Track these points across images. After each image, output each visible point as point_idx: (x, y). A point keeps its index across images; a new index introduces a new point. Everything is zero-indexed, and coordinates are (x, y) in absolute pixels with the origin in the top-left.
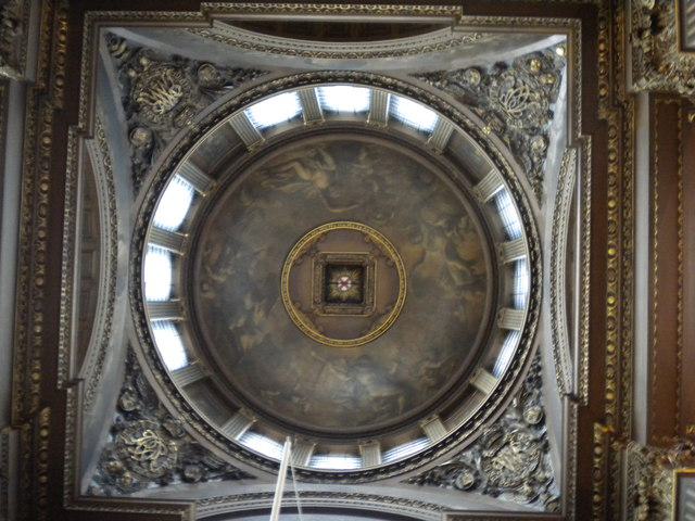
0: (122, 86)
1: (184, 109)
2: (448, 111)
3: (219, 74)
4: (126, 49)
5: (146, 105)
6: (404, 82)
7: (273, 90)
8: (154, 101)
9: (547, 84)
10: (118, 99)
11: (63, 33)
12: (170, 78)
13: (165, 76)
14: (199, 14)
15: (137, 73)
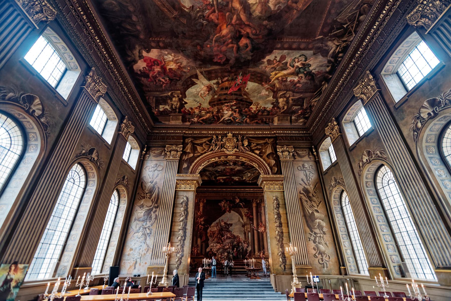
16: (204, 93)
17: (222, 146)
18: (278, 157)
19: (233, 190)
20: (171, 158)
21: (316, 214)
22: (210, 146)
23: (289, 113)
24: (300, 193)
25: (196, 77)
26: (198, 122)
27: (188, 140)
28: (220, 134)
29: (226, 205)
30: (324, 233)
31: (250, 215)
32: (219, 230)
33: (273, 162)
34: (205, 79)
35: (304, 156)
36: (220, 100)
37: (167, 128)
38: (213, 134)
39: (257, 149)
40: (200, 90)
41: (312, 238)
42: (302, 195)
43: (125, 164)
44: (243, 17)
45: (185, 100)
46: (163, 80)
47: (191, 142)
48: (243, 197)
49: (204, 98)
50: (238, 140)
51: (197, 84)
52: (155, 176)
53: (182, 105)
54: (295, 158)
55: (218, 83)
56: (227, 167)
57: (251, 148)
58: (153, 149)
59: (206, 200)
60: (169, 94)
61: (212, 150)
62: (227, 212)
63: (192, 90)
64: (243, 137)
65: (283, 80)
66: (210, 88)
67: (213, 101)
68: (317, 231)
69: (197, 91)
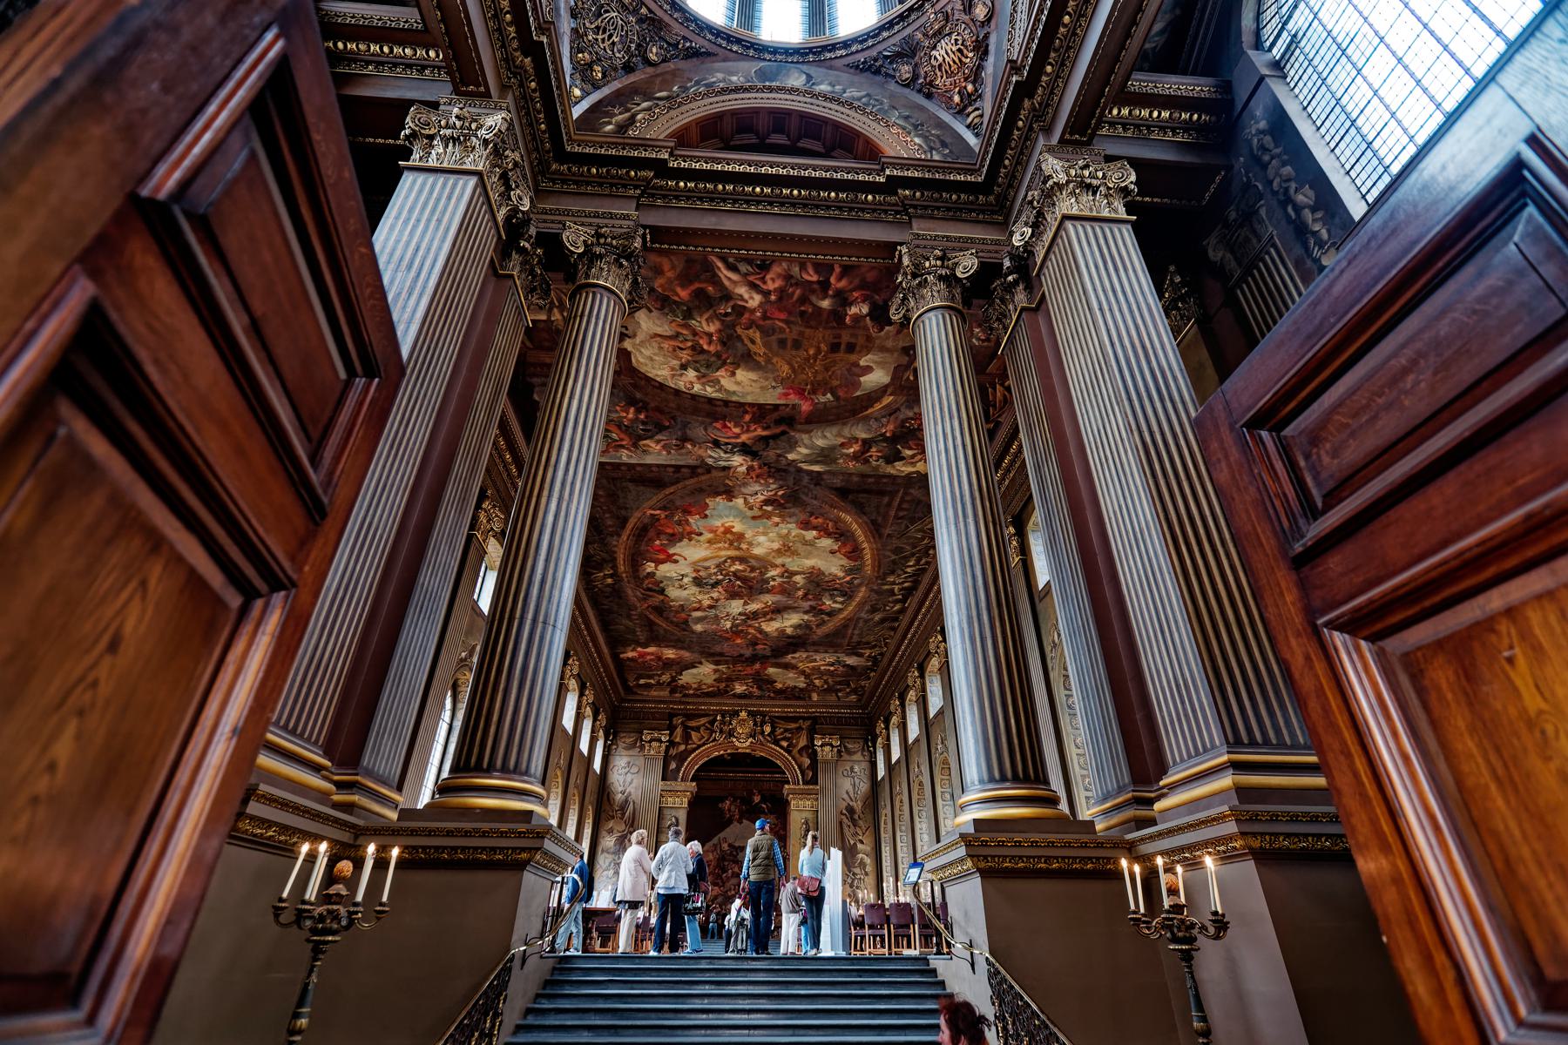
0: (983, 74)
1: (934, 35)
2: (676, 10)
3: (894, 70)
4: (968, 115)
5: (966, 47)
6: (720, 46)
7: (846, 44)
8: (960, 50)
9: (583, 52)
10: (991, 59)
11: (1005, 167)
12: (939, 74)
13: (942, 77)
14: (888, 172)
15: (965, 87)
17: (731, 734)
18: (815, 752)
20: (652, 752)
21: (859, 846)
22: (713, 732)
23: (830, 690)
24: (841, 813)
25: (701, 663)
26: (693, 696)
27: (678, 721)
28: (728, 711)
29: (733, 808)
30: (866, 874)
31: (780, 828)
32: (718, 859)
33: (807, 762)
35: (855, 753)
37: (645, 701)
38: (717, 710)
39: (784, 739)
41: (849, 881)
42: (843, 817)
43: (595, 772)
44: (758, 635)
47: (682, 723)
50: (755, 724)
52: (627, 783)
53: (674, 679)
54: (841, 756)
57: (775, 736)
58: (622, 735)
61: (715, 740)
62: (736, 823)
63: (694, 671)
64: (764, 716)
65: (816, 670)
66: (716, 671)
68: (857, 870)
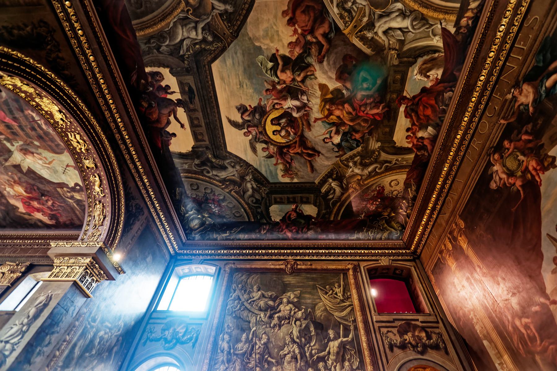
16: (41, 159)
19: (479, 102)
25: (17, 167)
29: (511, 164)
34: (13, 156)
36: (40, 138)
40: (37, 164)
45: (72, 185)
46: (50, 203)
48: (525, 60)
49: (50, 160)
51: (29, 167)
55: (8, 140)
56: (316, 113)
59: (461, 216)
60: (70, 201)
63: (45, 173)
66: (25, 151)
67: (49, 148)
69: (41, 168)
